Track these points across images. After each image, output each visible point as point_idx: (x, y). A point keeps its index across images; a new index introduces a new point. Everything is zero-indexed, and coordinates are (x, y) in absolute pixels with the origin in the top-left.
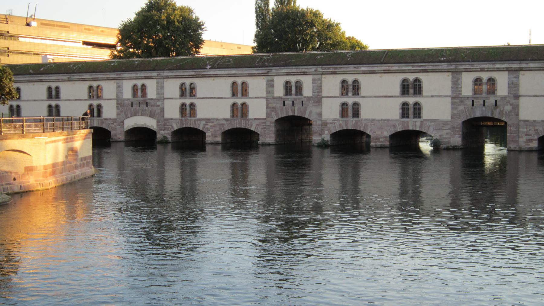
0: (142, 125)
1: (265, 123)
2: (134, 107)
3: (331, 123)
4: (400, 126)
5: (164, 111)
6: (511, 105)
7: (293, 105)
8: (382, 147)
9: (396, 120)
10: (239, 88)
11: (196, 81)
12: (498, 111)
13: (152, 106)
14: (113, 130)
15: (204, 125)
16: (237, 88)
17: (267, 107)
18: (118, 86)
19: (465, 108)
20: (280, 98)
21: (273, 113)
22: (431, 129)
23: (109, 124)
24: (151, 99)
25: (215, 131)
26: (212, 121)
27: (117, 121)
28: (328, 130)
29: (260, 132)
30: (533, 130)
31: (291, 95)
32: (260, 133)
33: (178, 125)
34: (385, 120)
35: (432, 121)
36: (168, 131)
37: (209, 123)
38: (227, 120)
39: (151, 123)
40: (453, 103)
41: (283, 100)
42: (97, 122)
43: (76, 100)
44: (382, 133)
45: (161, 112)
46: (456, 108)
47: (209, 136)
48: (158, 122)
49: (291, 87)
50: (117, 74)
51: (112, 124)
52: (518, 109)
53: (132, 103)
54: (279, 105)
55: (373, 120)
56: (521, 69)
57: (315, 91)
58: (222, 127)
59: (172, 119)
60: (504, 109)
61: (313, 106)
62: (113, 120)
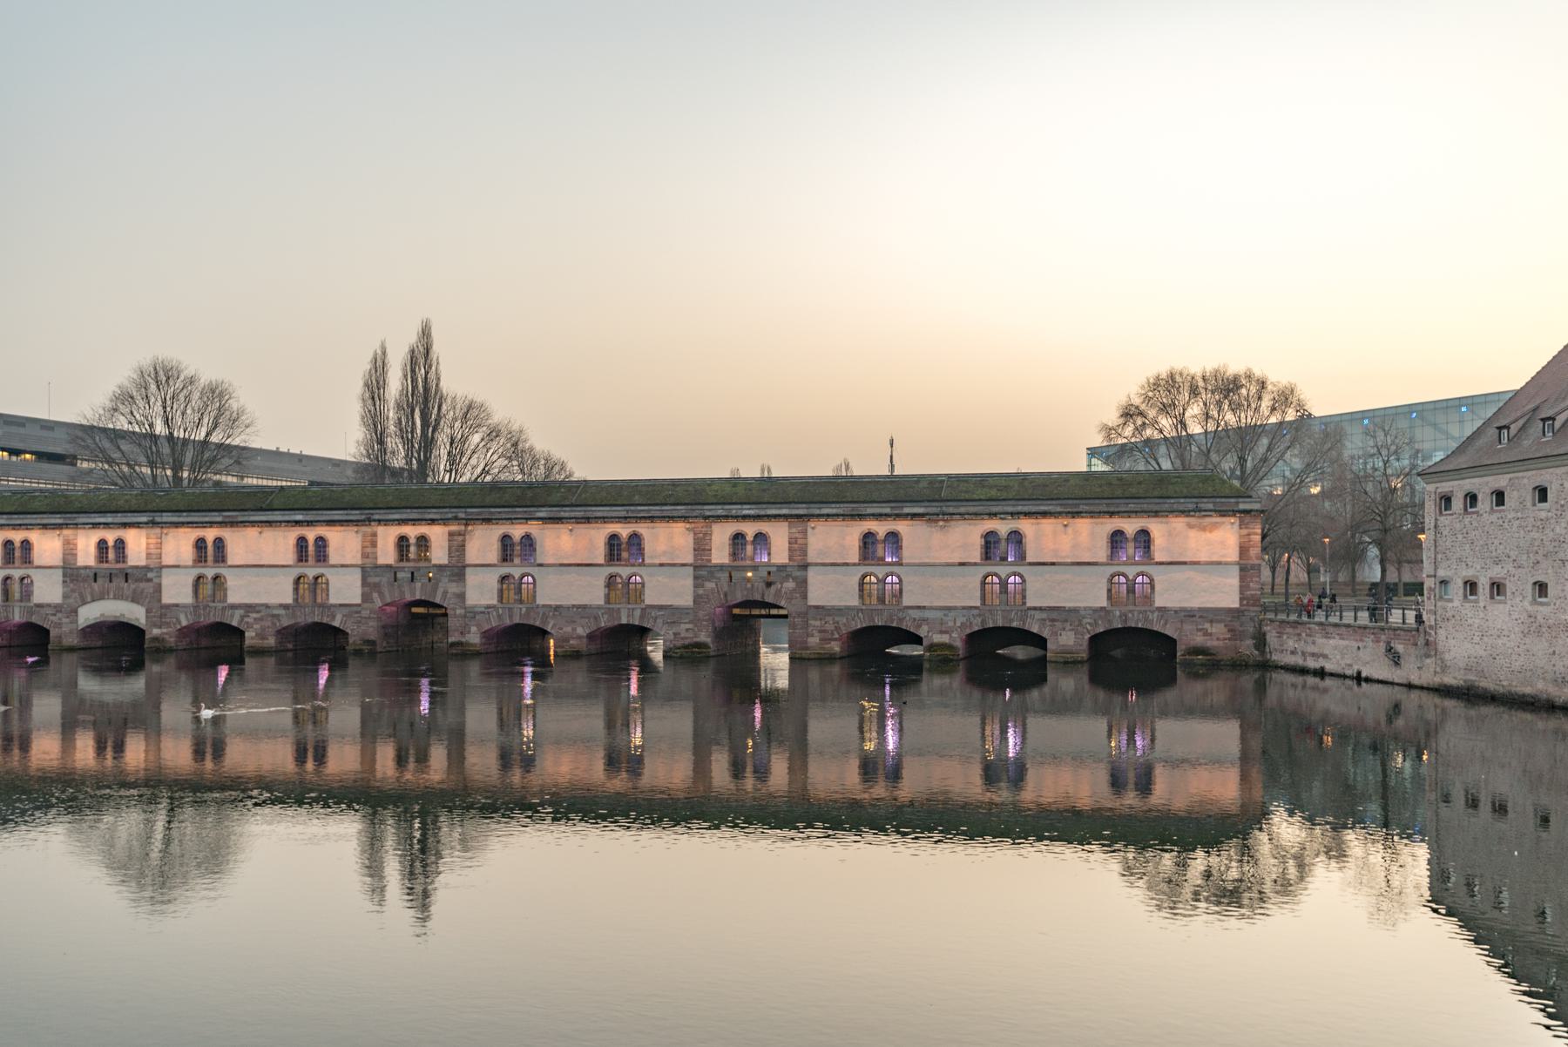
0: (116, 617)
1: (359, 612)
2: (99, 580)
3: (484, 612)
4: (606, 616)
5: (160, 592)
6: (794, 579)
7: (412, 580)
8: (575, 655)
9: (599, 607)
10: (311, 548)
12: (773, 589)
13: (136, 581)
14: (54, 627)
15: (241, 616)
16: (307, 547)
17: (364, 583)
18: (67, 543)
19: (717, 585)
20: (389, 566)
21: (375, 595)
22: (659, 621)
23: (47, 614)
24: (137, 567)
25: (263, 629)
26: (257, 609)
27: (63, 610)
28: (476, 625)
29: (352, 630)
30: (831, 622)
31: (408, 560)
32: (350, 632)
33: (189, 616)
34: (579, 607)
35: (661, 608)
36: (170, 629)
37: (251, 612)
38: (286, 607)
39: (135, 613)
40: (696, 578)
41: (393, 570)
45: (155, 591)
46: (703, 586)
47: (252, 638)
48: (147, 611)
49: (408, 546)
52: (806, 587)
53: (95, 574)
54: (385, 579)
55: (557, 608)
56: (810, 517)
57: (453, 555)
58: (276, 621)
59: (177, 605)
60: (781, 587)
61: (450, 581)
62: (55, 607)
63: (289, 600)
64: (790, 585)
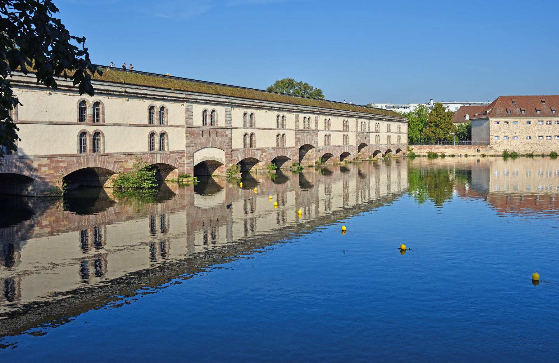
0: (211, 157)
2: (205, 135)
3: (321, 149)
11: (255, 111)
17: (296, 138)
18: (187, 110)
21: (299, 143)
23: (177, 158)
24: (222, 128)
33: (242, 156)
37: (264, 152)
38: (274, 149)
40: (356, 136)
42: (161, 157)
43: (131, 125)
44: (338, 155)
45: (229, 142)
48: (226, 154)
50: (186, 94)
51: (179, 158)
55: (335, 146)
59: (237, 150)
63: (275, 146)
64: (368, 138)
